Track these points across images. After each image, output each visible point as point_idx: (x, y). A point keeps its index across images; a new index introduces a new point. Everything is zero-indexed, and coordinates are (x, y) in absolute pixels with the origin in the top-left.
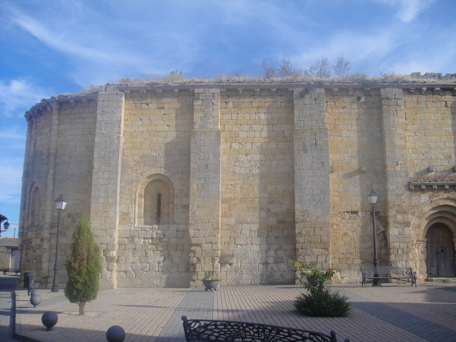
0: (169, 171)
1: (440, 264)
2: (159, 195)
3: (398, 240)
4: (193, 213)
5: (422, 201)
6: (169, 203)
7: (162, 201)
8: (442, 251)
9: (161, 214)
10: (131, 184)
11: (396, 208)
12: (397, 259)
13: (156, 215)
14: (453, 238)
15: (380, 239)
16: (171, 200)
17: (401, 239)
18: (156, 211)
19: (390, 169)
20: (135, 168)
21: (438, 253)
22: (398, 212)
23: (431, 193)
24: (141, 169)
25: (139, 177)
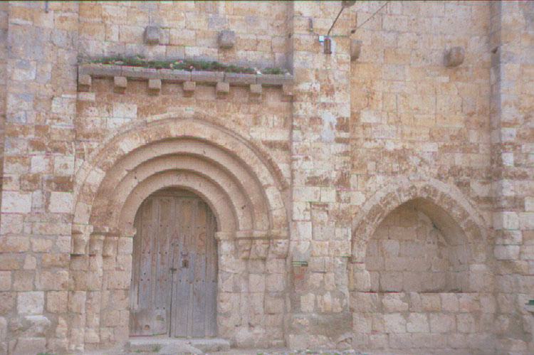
3: (27, 230)
5: (117, 120)
8: (185, 264)
11: (31, 136)
14: (216, 230)
17: (37, 225)
19: (19, 21)
22: (37, 145)
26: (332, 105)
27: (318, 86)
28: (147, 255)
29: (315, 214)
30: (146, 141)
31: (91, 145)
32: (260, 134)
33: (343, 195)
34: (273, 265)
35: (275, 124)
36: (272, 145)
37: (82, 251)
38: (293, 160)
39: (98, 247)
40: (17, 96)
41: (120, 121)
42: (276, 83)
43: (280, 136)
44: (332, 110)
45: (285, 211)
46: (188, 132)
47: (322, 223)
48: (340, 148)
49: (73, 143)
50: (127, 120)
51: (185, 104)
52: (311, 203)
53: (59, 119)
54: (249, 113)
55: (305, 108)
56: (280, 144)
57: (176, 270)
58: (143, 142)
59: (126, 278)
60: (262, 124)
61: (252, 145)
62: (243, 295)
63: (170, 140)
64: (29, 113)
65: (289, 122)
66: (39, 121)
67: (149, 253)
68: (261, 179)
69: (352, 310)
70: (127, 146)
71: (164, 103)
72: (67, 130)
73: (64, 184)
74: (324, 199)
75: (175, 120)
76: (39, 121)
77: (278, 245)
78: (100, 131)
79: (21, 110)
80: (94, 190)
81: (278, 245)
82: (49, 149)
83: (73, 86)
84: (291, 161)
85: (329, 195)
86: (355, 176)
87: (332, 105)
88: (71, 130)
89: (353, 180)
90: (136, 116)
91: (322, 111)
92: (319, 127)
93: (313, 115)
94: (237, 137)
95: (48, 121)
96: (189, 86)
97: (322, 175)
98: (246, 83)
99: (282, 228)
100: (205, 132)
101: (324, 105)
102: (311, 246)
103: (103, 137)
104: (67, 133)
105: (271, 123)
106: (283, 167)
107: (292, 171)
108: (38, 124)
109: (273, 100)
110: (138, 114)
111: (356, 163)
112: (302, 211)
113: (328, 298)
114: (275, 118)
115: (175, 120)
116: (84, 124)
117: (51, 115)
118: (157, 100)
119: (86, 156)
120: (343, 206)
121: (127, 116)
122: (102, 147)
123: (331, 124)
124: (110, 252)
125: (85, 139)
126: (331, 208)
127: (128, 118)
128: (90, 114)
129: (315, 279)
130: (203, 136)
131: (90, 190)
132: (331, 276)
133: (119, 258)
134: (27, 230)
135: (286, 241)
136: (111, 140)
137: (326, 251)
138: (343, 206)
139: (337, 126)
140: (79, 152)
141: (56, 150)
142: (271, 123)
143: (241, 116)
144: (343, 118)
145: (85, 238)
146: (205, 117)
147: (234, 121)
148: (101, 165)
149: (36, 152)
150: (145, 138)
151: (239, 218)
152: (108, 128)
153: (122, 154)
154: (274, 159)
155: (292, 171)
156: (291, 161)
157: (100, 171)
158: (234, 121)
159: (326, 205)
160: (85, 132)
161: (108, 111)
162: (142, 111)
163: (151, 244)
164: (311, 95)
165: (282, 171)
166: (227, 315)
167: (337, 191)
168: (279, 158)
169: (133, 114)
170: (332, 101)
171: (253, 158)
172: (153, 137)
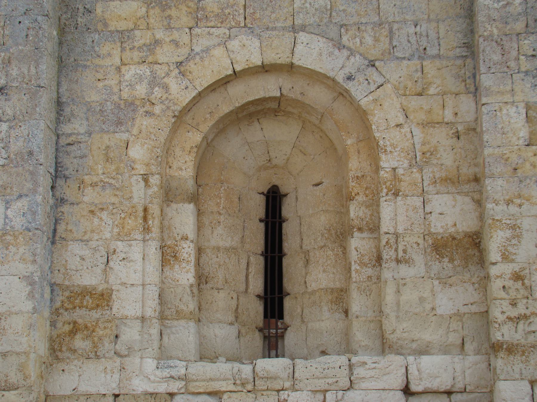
0: (340, 47)
2: (274, 199)
4: (517, 277)
6: (341, 235)
7: (289, 229)
9: (288, 303)
10: (119, 123)
13: (259, 307)
16: (356, 211)
18: (257, 284)
20: (142, 38)
24: (176, 43)
25: (166, 88)
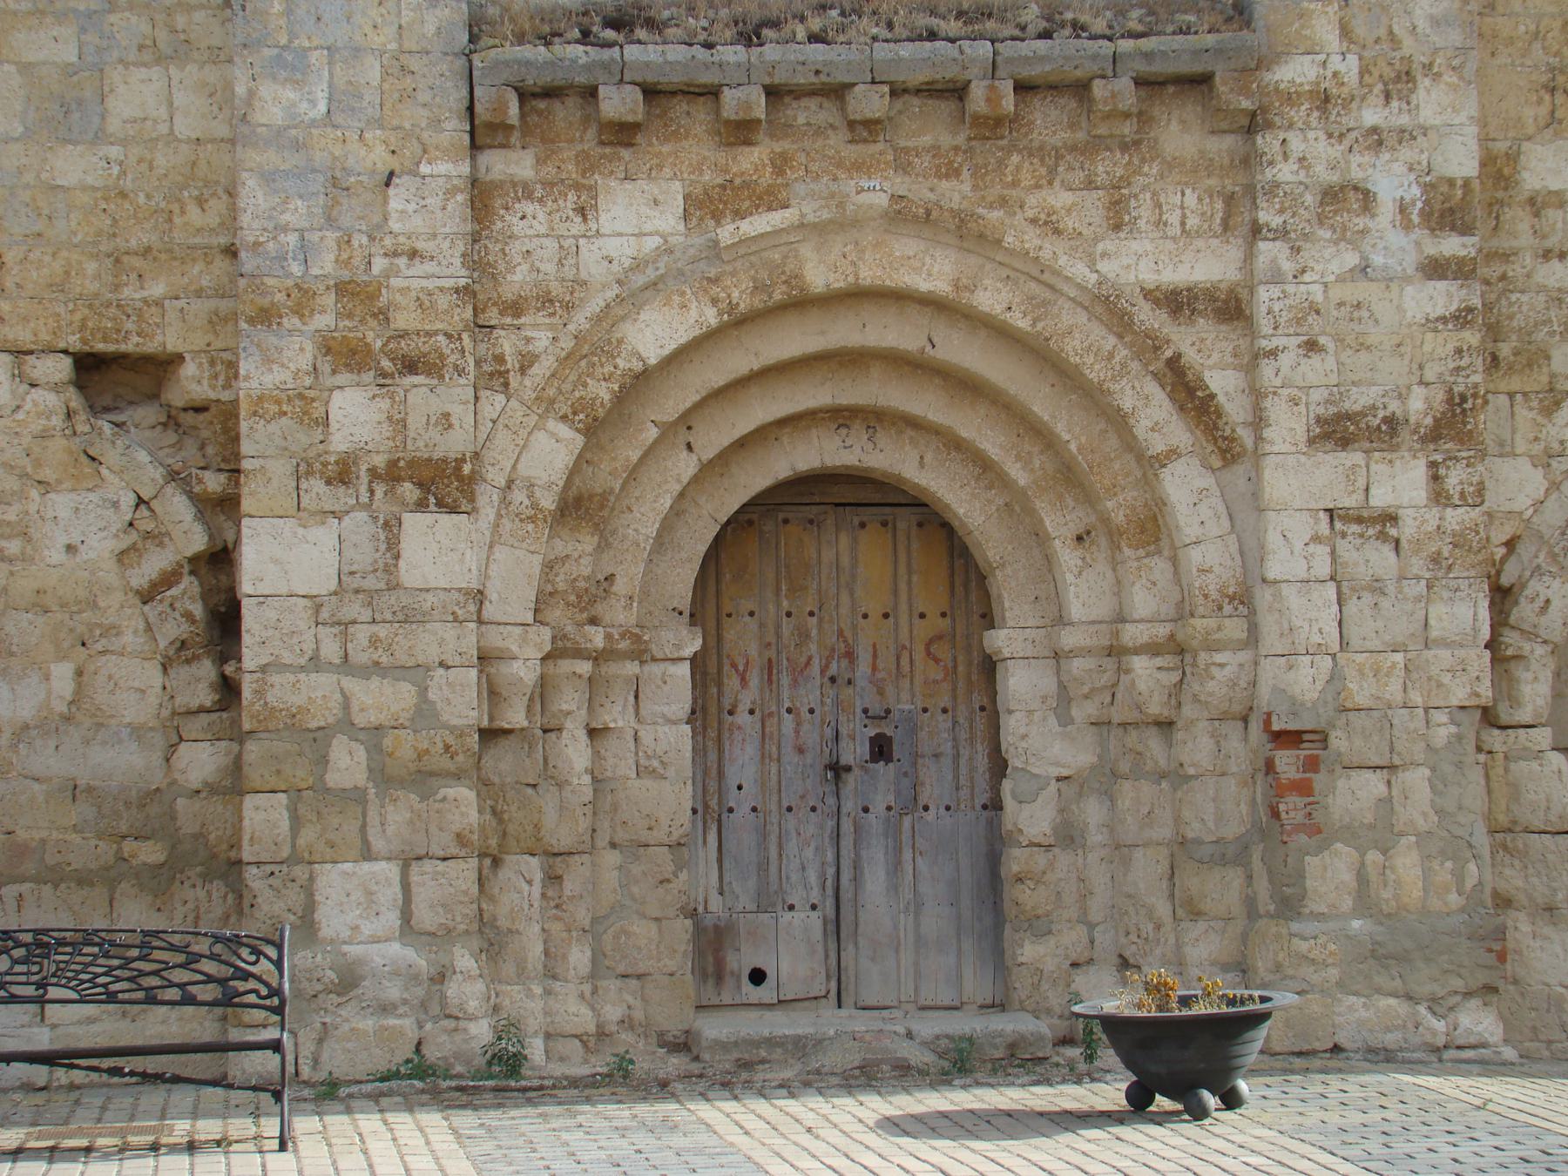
1: (856, 880)
3: (331, 650)
5: (612, 246)
8: (881, 749)
11: (324, 321)
12: (308, 835)
14: (989, 620)
15: (172, 630)
17: (362, 634)
21: (837, 770)
22: (346, 355)
23: (694, 155)
26: (1405, 135)
27: (1349, 67)
28: (742, 718)
29: (1345, 548)
30: (720, 314)
31: (528, 340)
32: (1139, 263)
33: (1454, 478)
34: (1197, 748)
35: (1193, 222)
36: (1178, 302)
37: (515, 717)
38: (1257, 356)
39: (570, 701)
40: (268, 178)
41: (623, 250)
42: (1186, 67)
43: (1210, 266)
44: (1406, 153)
45: (1234, 548)
46: (869, 275)
47: (1376, 587)
48: (1442, 297)
49: (465, 336)
50: (652, 243)
51: (858, 167)
52: (1330, 511)
53: (413, 254)
54: (1090, 185)
55: (1302, 155)
56: (1210, 294)
57: (848, 769)
58: (711, 317)
59: (669, 800)
60: (1142, 223)
61: (1109, 307)
62: (1093, 857)
63: (802, 303)
64: (314, 237)
65: (1239, 215)
66: (347, 263)
67: (752, 712)
68: (1141, 429)
69: (1503, 902)
70: (653, 334)
71: (779, 171)
72: (441, 289)
73: (443, 484)
74: (1381, 498)
75: (818, 230)
76: (347, 263)
77: (1215, 671)
78: (556, 289)
79: (285, 229)
80: (548, 502)
81: (1215, 671)
82: (386, 364)
83: (454, 130)
84: (1252, 361)
85: (1400, 483)
86: (1503, 400)
87: (1405, 135)
88: (457, 291)
89: (1489, 422)
90: (681, 227)
91: (1367, 158)
92: (1361, 222)
93: (1335, 178)
94: (1042, 274)
95: (379, 264)
96: (869, 102)
97: (1374, 407)
98: (1079, 73)
99: (1228, 609)
100: (933, 270)
101: (1376, 139)
102: (1335, 676)
103: (568, 307)
104: (443, 302)
105: (1174, 218)
106: (1222, 382)
107: (1257, 395)
108: (346, 275)
109: (1181, 133)
110: (686, 216)
111: (1505, 350)
112: (1298, 546)
113: (1407, 863)
114: (1191, 199)
115: (818, 230)
116: (502, 267)
117: (388, 241)
118: (752, 160)
119: (513, 383)
120: (1455, 518)
121: (648, 228)
122: (567, 344)
123: (1403, 209)
124: (616, 715)
125: (508, 320)
126: (1407, 529)
127: (650, 234)
128: (519, 227)
129: (1352, 795)
130: (924, 286)
131: (535, 506)
132: (1417, 779)
133: (646, 736)
134: (331, 650)
135: (1244, 656)
136: (598, 319)
137: (1393, 690)
138: (1455, 518)
139: (1426, 215)
140: (487, 368)
141: (410, 366)
142: (1174, 218)
143: (1060, 198)
144: (1451, 182)
145: (523, 671)
146: (928, 213)
147: (1034, 221)
148: (566, 410)
149: (343, 378)
150: (715, 301)
151: (1070, 578)
152: (583, 275)
153: (638, 366)
154: (1191, 356)
155: (1257, 395)
156: (1252, 361)
157: (564, 431)
158: (1034, 221)
159: (1391, 518)
160: (508, 293)
161: (581, 211)
162: (706, 206)
163: (754, 680)
164: (1323, 101)
165: (1221, 399)
166: (1039, 926)
167: (1433, 465)
168: (1207, 351)
169: (668, 220)
170: (1404, 120)
171: (1111, 356)
172: (741, 296)
